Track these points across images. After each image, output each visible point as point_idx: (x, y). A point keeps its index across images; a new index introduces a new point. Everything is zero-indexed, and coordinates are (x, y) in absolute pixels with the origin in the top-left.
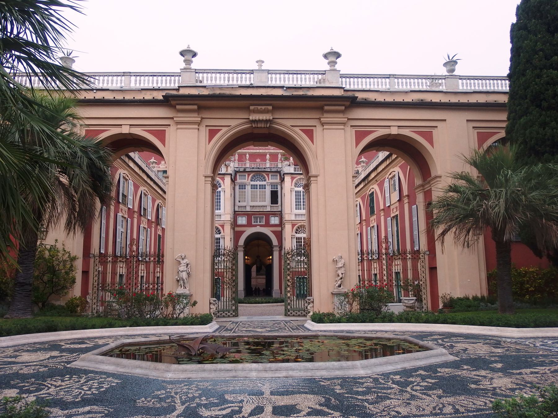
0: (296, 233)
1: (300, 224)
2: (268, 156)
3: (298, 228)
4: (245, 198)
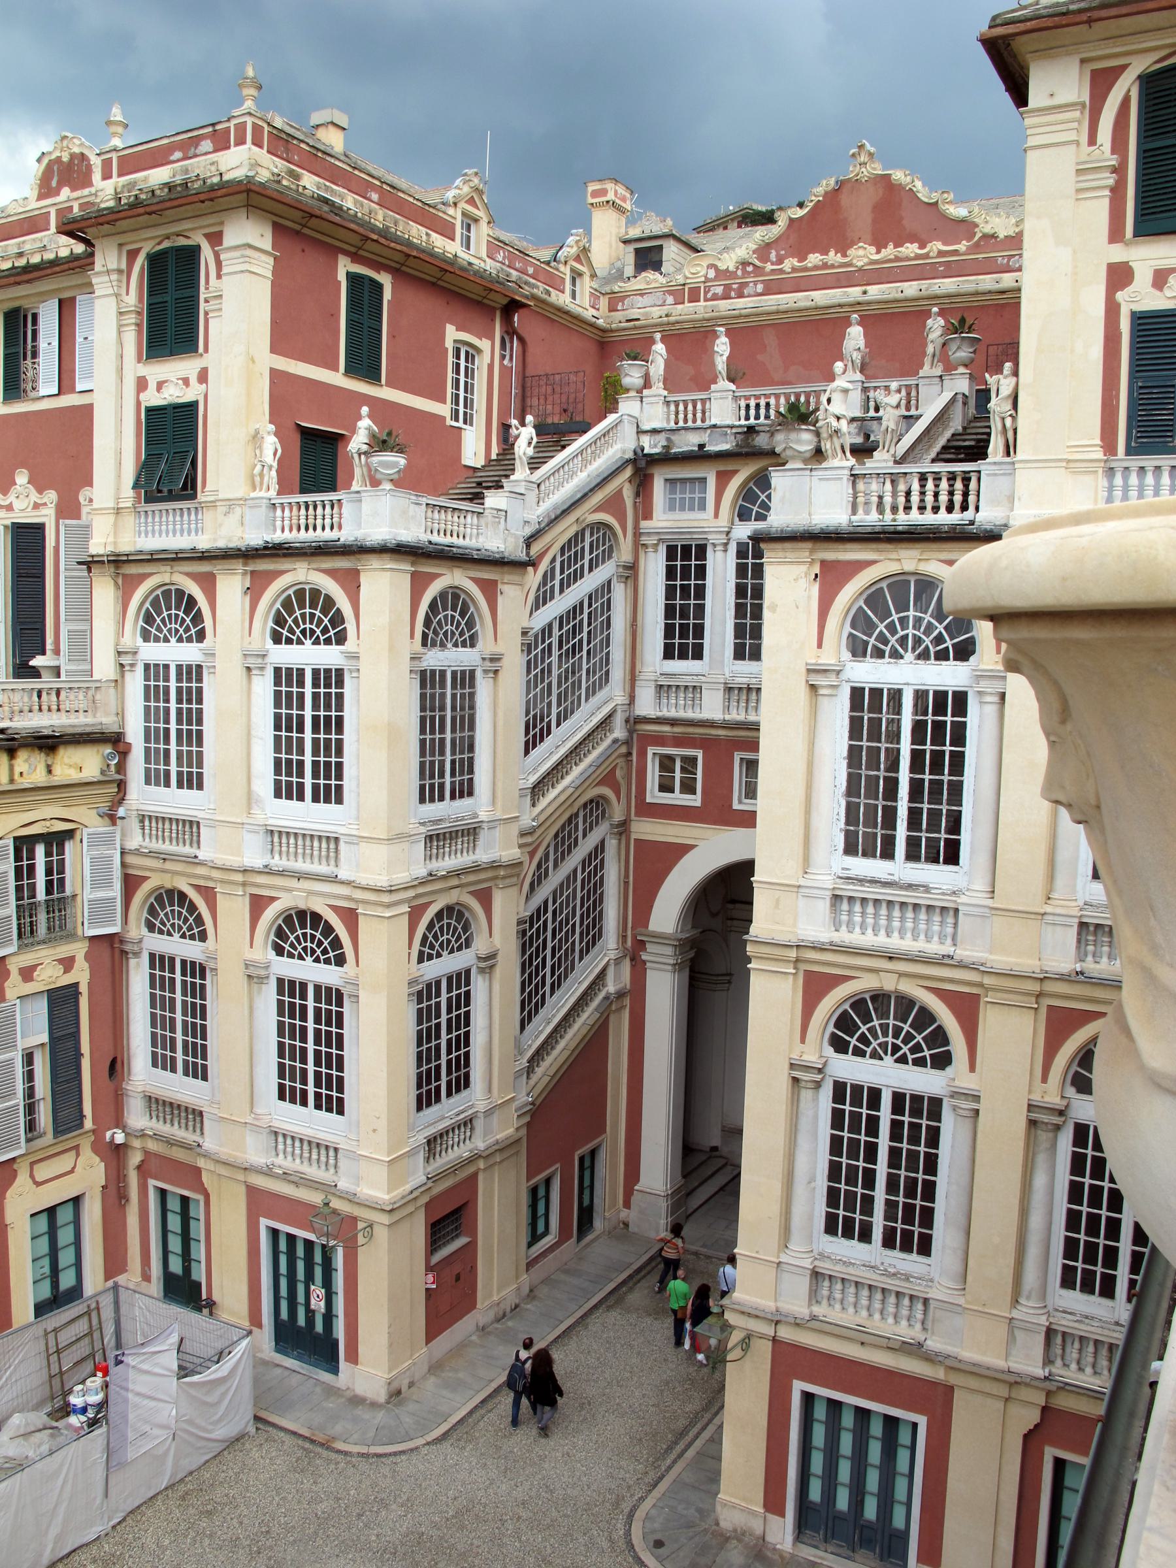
0: (840, 1046)
1: (864, 984)
2: (855, 337)
3: (859, 1004)
4: (699, 631)
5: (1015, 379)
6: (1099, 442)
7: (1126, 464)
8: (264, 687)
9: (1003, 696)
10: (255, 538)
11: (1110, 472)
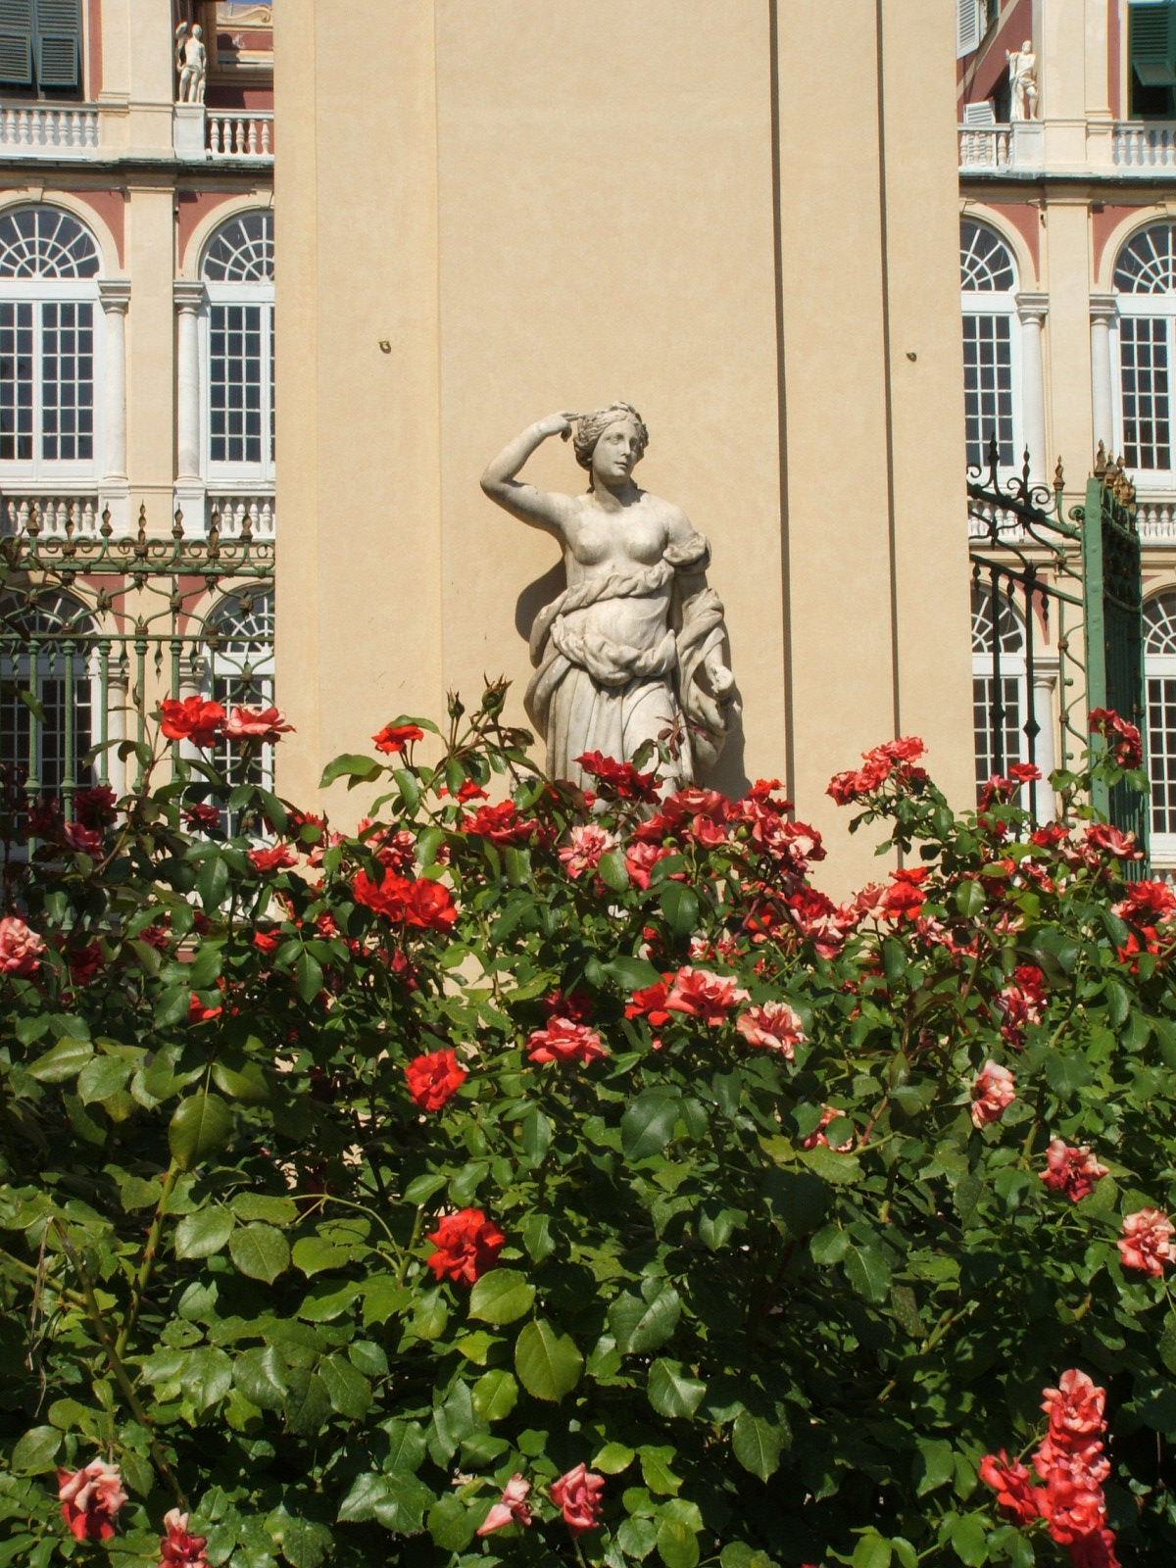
5: (1032, 58)
6: (1106, 108)
7: (1129, 128)
8: (197, 331)
9: (1042, 318)
10: (191, 149)
11: (1116, 133)
